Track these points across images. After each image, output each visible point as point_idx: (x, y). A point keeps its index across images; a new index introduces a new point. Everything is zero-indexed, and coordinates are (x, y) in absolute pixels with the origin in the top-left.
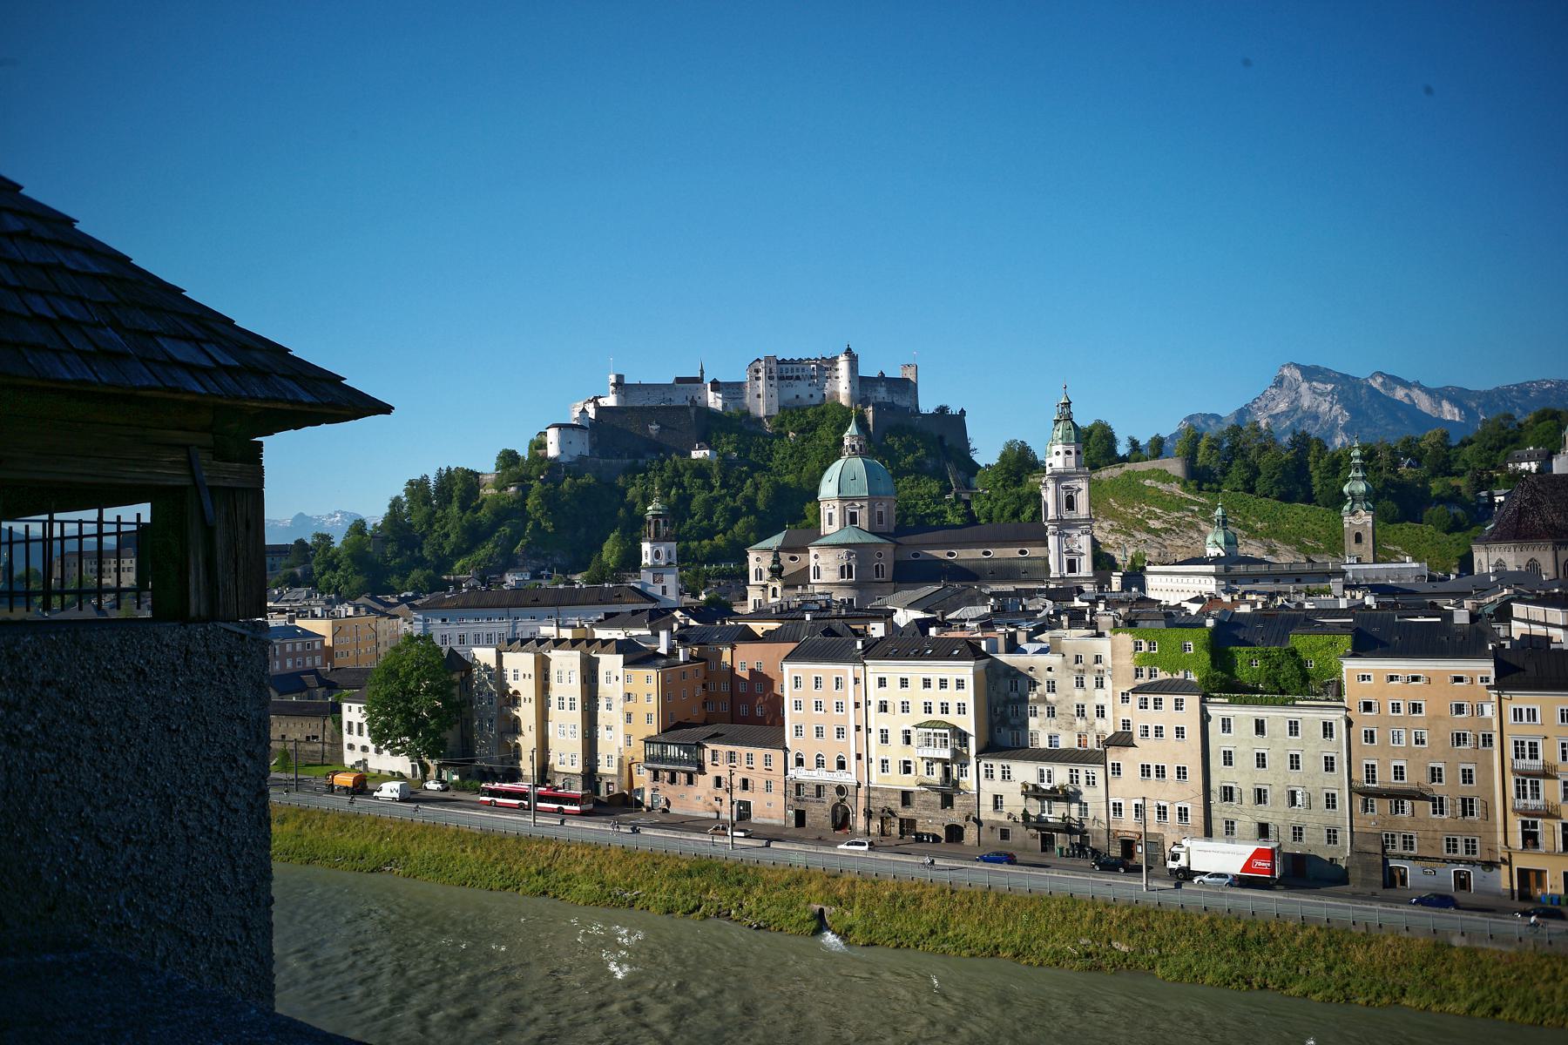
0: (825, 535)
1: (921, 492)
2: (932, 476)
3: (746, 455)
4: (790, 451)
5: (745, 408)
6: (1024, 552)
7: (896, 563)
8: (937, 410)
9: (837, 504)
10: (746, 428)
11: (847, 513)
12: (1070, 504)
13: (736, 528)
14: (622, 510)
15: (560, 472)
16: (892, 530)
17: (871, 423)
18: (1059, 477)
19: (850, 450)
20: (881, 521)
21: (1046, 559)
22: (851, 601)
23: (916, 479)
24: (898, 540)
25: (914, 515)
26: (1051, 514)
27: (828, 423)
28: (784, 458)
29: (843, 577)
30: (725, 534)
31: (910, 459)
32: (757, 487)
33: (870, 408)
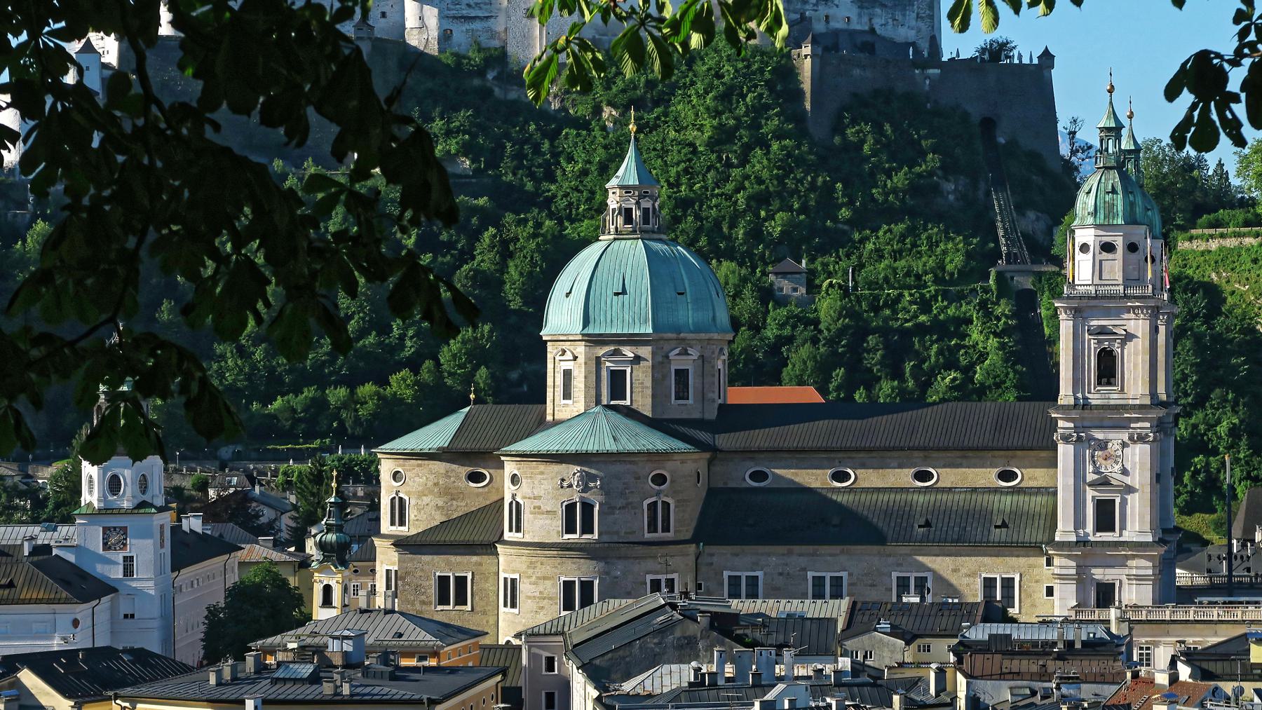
0: (556, 423)
1: (918, 266)
2: (953, 224)
3: (494, 163)
4: (599, 155)
5: (496, 43)
6: (1007, 476)
7: (712, 492)
8: (983, 50)
9: (580, 349)
10: (497, 91)
11: (605, 375)
12: (1108, 369)
13: (445, 355)
14: (166, 305)
15: (22, 205)
16: (712, 414)
17: (807, 86)
18: (1084, 307)
19: (620, 220)
20: (682, 394)
21: (1055, 493)
22: (587, 587)
23: (912, 231)
24: (724, 441)
25: (884, 332)
26: (1066, 394)
27: (700, 86)
28: (584, 173)
29: (570, 528)
30: (416, 370)
31: (899, 179)
32: (505, 250)
33: (807, 50)
